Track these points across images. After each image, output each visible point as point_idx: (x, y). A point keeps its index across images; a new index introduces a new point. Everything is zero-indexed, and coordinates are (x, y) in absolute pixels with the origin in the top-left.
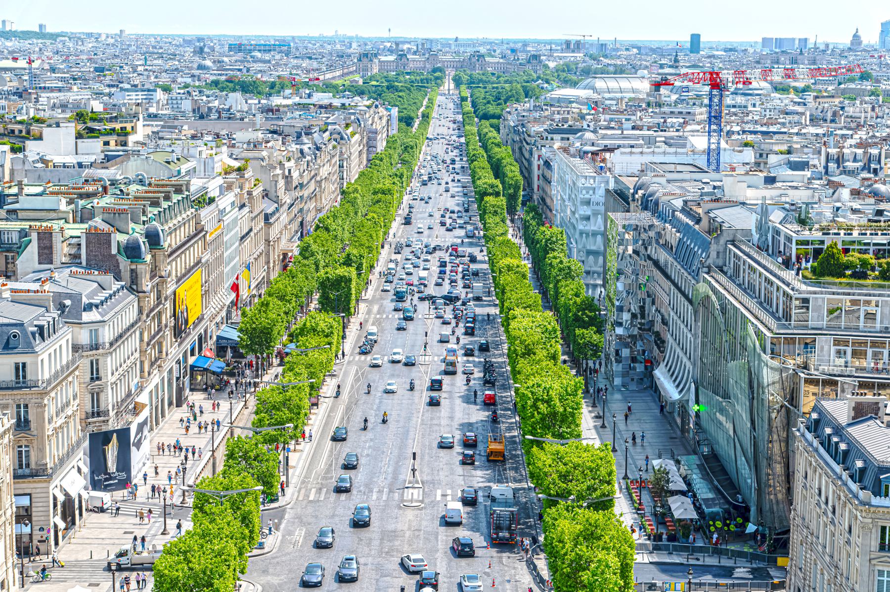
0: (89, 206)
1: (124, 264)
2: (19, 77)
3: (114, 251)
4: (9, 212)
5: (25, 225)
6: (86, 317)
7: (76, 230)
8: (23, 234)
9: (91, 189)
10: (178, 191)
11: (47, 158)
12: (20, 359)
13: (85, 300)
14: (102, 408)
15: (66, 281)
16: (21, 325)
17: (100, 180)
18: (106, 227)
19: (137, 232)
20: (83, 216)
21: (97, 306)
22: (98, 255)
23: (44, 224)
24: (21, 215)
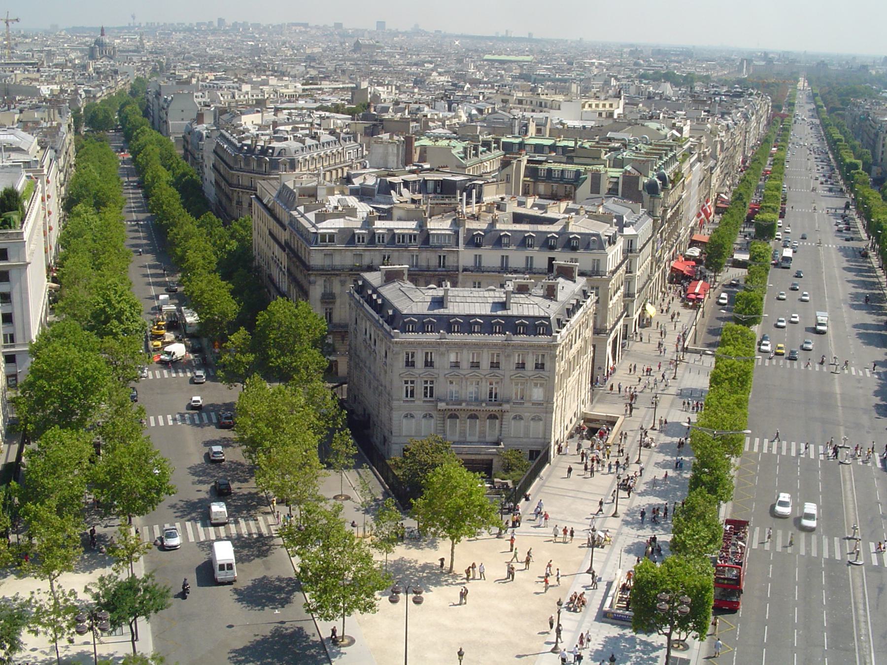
0: (620, 157)
1: (646, 195)
2: (521, 67)
3: (641, 188)
4: (568, 157)
5: (582, 168)
6: (628, 231)
7: (616, 173)
8: (578, 173)
9: (617, 145)
10: (671, 150)
11: (564, 122)
12: (596, 257)
13: (625, 219)
14: (631, 292)
15: (613, 205)
16: (598, 235)
17: (623, 139)
18: (634, 172)
19: (652, 176)
20: (619, 164)
21: (632, 224)
22: (629, 189)
23: (594, 168)
24: (576, 160)
